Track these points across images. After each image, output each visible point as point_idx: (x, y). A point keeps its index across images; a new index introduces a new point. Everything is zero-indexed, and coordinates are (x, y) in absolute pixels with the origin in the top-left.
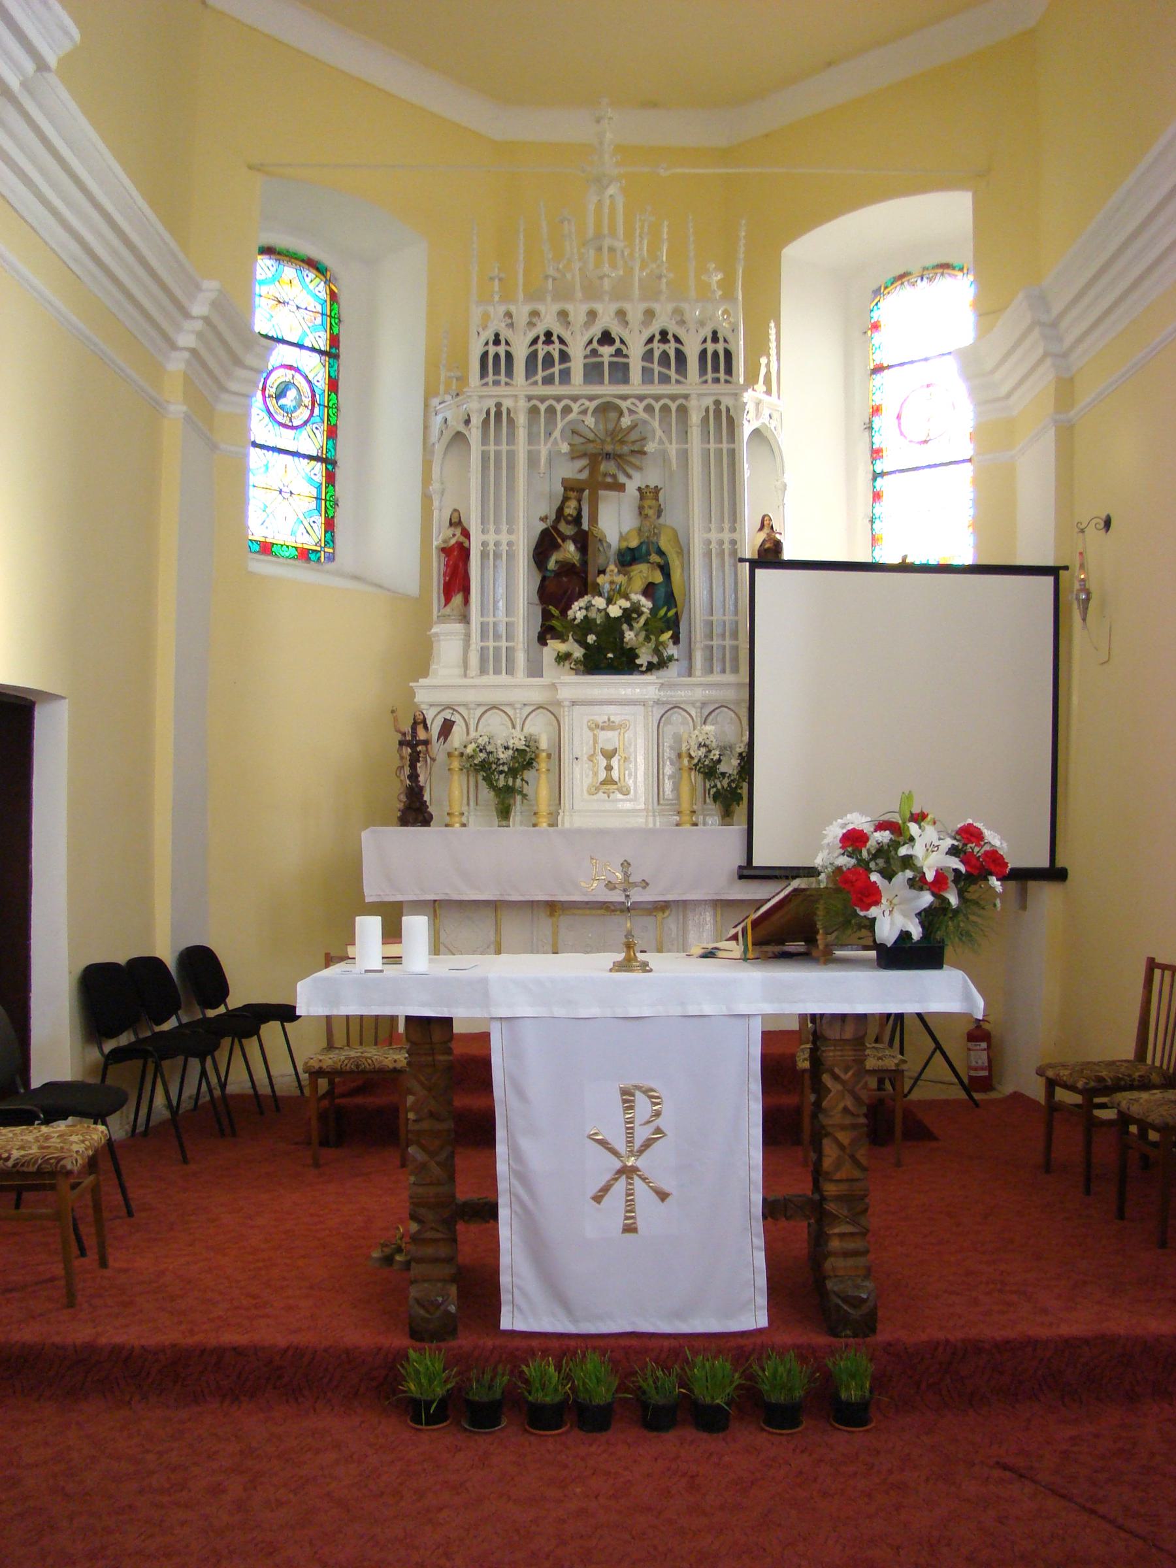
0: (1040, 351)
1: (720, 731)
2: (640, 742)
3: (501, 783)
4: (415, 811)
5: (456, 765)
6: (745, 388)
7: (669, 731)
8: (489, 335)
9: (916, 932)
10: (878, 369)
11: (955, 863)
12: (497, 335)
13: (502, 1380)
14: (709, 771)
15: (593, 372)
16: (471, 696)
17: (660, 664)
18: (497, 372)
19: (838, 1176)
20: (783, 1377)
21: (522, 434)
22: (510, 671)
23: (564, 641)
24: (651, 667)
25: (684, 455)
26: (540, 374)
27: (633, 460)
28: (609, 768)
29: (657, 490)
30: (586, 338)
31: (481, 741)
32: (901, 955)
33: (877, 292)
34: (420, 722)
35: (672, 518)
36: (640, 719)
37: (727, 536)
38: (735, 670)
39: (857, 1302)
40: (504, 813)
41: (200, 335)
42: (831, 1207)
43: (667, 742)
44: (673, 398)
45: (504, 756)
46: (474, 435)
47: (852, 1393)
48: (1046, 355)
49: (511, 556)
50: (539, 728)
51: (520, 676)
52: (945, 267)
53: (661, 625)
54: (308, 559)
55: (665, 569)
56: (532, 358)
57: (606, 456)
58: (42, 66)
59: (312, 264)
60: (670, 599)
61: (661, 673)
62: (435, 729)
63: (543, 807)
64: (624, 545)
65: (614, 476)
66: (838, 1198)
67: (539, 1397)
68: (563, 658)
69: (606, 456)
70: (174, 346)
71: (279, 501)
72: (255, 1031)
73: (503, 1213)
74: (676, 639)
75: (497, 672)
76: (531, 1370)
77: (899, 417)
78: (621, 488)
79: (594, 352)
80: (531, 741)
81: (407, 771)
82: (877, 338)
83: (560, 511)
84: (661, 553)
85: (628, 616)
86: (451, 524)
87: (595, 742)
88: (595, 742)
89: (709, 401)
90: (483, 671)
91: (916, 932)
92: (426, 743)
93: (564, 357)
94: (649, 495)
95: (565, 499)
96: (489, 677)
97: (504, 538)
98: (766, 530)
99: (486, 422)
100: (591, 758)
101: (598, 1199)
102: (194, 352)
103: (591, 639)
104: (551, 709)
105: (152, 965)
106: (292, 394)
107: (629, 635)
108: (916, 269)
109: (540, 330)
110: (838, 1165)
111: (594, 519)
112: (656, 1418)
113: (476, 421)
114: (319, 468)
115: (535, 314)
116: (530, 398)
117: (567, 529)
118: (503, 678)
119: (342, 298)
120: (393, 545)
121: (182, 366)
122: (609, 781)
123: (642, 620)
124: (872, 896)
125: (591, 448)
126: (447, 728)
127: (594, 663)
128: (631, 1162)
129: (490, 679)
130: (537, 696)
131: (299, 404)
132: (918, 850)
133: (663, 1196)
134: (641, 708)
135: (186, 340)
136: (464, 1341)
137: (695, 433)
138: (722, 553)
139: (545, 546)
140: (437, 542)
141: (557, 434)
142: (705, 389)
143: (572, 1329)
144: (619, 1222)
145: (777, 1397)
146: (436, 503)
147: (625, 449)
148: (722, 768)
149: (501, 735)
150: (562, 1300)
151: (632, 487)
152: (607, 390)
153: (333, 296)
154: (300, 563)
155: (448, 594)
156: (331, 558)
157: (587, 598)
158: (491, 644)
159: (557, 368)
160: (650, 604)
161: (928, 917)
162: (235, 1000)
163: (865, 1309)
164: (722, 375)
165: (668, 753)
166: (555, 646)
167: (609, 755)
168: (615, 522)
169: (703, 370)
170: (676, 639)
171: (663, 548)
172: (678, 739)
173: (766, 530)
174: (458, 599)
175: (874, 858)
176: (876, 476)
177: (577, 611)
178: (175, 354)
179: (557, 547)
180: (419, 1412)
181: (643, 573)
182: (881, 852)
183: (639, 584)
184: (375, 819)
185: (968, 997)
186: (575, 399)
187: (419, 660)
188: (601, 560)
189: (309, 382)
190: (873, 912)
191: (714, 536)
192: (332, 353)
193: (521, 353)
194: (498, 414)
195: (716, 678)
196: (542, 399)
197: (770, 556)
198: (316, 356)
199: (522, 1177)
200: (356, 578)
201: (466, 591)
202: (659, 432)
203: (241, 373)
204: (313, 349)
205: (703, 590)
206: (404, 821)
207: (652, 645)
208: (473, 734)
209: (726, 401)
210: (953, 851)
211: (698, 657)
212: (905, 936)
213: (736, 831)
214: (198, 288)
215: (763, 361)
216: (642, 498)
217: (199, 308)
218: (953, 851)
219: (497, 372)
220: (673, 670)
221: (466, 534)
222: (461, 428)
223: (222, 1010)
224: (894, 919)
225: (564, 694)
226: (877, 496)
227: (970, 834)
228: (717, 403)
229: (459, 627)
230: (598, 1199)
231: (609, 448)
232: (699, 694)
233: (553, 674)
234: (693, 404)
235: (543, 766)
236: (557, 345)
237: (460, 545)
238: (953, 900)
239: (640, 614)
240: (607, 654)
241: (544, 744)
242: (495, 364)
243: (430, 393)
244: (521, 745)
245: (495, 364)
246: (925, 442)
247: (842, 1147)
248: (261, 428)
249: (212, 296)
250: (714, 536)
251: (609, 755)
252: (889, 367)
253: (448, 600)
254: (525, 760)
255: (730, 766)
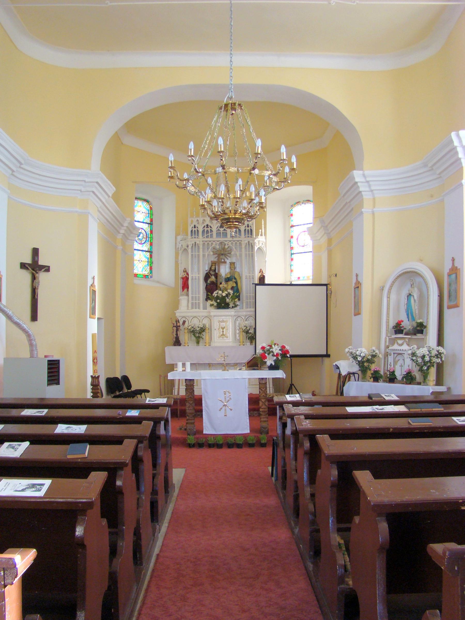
0: (323, 232)
1: (250, 322)
2: (231, 325)
3: (197, 335)
4: (177, 342)
5: (186, 331)
6: (256, 238)
7: (237, 322)
8: (193, 226)
9: (273, 364)
10: (292, 226)
11: (280, 352)
12: (195, 226)
13: (204, 440)
14: (247, 332)
15: (218, 234)
16: (189, 314)
17: (236, 306)
18: (195, 235)
19: (263, 407)
20: (252, 439)
21: (201, 250)
22: (199, 308)
23: (212, 301)
24: (233, 307)
25: (241, 255)
26: (205, 235)
27: (228, 255)
28: (223, 332)
29: (234, 263)
30: (217, 226)
31: (193, 326)
32: (272, 368)
33: (292, 206)
34: (178, 321)
35: (238, 270)
36: (231, 320)
37: (251, 275)
38: (253, 308)
39: (265, 428)
40: (198, 343)
41: (125, 230)
42: (261, 413)
43: (237, 324)
44: (238, 241)
45: (198, 329)
46: (190, 250)
47: (263, 442)
48: (325, 233)
49: (199, 279)
50: (206, 322)
51: (201, 309)
52: (309, 201)
53: (234, 297)
54: (146, 278)
55: (236, 283)
56: (203, 231)
57: (222, 254)
58: (109, 196)
59: (146, 200)
60: (238, 289)
61: (236, 308)
62: (181, 322)
63: (207, 341)
64: (226, 277)
65: (224, 259)
66: (263, 411)
67: (210, 442)
68: (212, 305)
69: (222, 254)
70: (119, 233)
71: (140, 265)
72: (141, 394)
73: (204, 413)
74: (239, 300)
75: (196, 308)
76: (209, 439)
77: (297, 239)
78: (225, 262)
79: (219, 230)
80: (204, 325)
81: (175, 333)
82: (292, 218)
83: (211, 268)
84: (235, 279)
85: (227, 295)
86: (184, 271)
87: (220, 325)
88: (220, 325)
89: (247, 242)
90: (192, 308)
91: (273, 364)
92: (179, 326)
93: (211, 231)
94: (232, 264)
95: (212, 266)
96: (194, 309)
97: (197, 275)
98: (261, 272)
99: (192, 247)
100: (219, 329)
101: (220, 410)
102: (124, 234)
103: (218, 301)
104: (209, 317)
105: (117, 378)
106: (141, 235)
107: (227, 300)
108: (302, 201)
109: (205, 224)
110: (262, 405)
111: (219, 270)
112: (230, 446)
113: (190, 247)
114: (148, 254)
115: (204, 220)
116: (203, 241)
117: (212, 273)
118: (197, 310)
119: (153, 209)
120: (168, 273)
121: (121, 237)
122: (223, 335)
123: (231, 296)
124: (265, 357)
125: (218, 253)
126: (184, 322)
127: (219, 307)
128: (225, 404)
129: (194, 310)
130: (205, 314)
131: (143, 237)
132: (274, 350)
133: (231, 410)
134: (230, 317)
135: (122, 231)
136: (197, 436)
137: (243, 250)
138: (250, 278)
139: (207, 277)
140: (180, 276)
141: (210, 250)
142: (245, 239)
143: (216, 433)
144: (223, 414)
145: (250, 442)
146: (180, 266)
147: (227, 252)
148: (250, 331)
149: (196, 324)
150: (213, 427)
151: (228, 261)
152: (222, 239)
153: (151, 208)
154: (144, 279)
155: (183, 289)
156: (151, 277)
157: (217, 291)
158: (194, 302)
159: (209, 234)
160: (232, 292)
161: (275, 361)
162: (133, 389)
163: (266, 429)
164: (250, 235)
165: (237, 328)
166: (209, 302)
167: (223, 328)
168: (224, 271)
169: (245, 234)
170: (239, 300)
171: (236, 277)
172: (239, 324)
173: (261, 272)
174: (186, 290)
175: (267, 351)
176: (292, 254)
177: (215, 294)
178: (119, 235)
179: (210, 277)
180: (190, 446)
181: (231, 284)
182: (268, 350)
183: (230, 287)
184: (168, 345)
185: (283, 375)
186: (214, 241)
187: (176, 305)
188: (221, 281)
189: (145, 232)
190: (266, 360)
191: (248, 275)
192: (151, 224)
193: (201, 230)
194: (195, 245)
195: (249, 310)
196: (206, 241)
197: (262, 281)
198: (147, 225)
199: (207, 406)
200: (158, 282)
201: (188, 288)
202: (235, 249)
203: (132, 235)
204: (146, 223)
205: (245, 287)
206: (175, 345)
207: (233, 302)
208: (190, 324)
209: (251, 242)
210: (280, 350)
211: (244, 304)
212: (271, 364)
213: (254, 345)
214: (126, 220)
215: (260, 231)
216: (231, 265)
217: (126, 224)
218: (280, 350)
219: (195, 235)
220: (238, 307)
221: (188, 274)
222: (186, 248)
223: (130, 391)
224: (270, 361)
225: (212, 314)
226: (292, 260)
227: (283, 347)
228: (249, 242)
229: (186, 297)
230: (220, 410)
231: (222, 252)
232: (244, 313)
233: (209, 308)
234: (243, 242)
235: (207, 331)
236: (210, 228)
237: (186, 277)
238: (280, 358)
239: (230, 295)
240: (222, 304)
241: (207, 326)
242: (194, 233)
243: (177, 235)
244: (202, 326)
245: (194, 233)
246: (303, 246)
247: (263, 402)
248: (137, 246)
249: (129, 221)
250: (248, 275)
251: (223, 328)
252: (295, 226)
253: (183, 290)
254: (203, 330)
255: (252, 331)
